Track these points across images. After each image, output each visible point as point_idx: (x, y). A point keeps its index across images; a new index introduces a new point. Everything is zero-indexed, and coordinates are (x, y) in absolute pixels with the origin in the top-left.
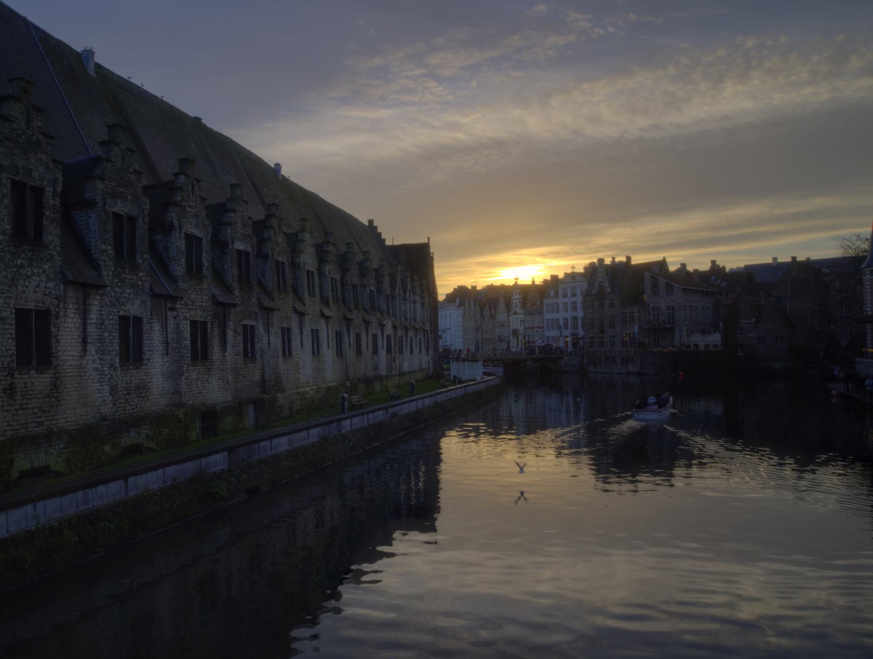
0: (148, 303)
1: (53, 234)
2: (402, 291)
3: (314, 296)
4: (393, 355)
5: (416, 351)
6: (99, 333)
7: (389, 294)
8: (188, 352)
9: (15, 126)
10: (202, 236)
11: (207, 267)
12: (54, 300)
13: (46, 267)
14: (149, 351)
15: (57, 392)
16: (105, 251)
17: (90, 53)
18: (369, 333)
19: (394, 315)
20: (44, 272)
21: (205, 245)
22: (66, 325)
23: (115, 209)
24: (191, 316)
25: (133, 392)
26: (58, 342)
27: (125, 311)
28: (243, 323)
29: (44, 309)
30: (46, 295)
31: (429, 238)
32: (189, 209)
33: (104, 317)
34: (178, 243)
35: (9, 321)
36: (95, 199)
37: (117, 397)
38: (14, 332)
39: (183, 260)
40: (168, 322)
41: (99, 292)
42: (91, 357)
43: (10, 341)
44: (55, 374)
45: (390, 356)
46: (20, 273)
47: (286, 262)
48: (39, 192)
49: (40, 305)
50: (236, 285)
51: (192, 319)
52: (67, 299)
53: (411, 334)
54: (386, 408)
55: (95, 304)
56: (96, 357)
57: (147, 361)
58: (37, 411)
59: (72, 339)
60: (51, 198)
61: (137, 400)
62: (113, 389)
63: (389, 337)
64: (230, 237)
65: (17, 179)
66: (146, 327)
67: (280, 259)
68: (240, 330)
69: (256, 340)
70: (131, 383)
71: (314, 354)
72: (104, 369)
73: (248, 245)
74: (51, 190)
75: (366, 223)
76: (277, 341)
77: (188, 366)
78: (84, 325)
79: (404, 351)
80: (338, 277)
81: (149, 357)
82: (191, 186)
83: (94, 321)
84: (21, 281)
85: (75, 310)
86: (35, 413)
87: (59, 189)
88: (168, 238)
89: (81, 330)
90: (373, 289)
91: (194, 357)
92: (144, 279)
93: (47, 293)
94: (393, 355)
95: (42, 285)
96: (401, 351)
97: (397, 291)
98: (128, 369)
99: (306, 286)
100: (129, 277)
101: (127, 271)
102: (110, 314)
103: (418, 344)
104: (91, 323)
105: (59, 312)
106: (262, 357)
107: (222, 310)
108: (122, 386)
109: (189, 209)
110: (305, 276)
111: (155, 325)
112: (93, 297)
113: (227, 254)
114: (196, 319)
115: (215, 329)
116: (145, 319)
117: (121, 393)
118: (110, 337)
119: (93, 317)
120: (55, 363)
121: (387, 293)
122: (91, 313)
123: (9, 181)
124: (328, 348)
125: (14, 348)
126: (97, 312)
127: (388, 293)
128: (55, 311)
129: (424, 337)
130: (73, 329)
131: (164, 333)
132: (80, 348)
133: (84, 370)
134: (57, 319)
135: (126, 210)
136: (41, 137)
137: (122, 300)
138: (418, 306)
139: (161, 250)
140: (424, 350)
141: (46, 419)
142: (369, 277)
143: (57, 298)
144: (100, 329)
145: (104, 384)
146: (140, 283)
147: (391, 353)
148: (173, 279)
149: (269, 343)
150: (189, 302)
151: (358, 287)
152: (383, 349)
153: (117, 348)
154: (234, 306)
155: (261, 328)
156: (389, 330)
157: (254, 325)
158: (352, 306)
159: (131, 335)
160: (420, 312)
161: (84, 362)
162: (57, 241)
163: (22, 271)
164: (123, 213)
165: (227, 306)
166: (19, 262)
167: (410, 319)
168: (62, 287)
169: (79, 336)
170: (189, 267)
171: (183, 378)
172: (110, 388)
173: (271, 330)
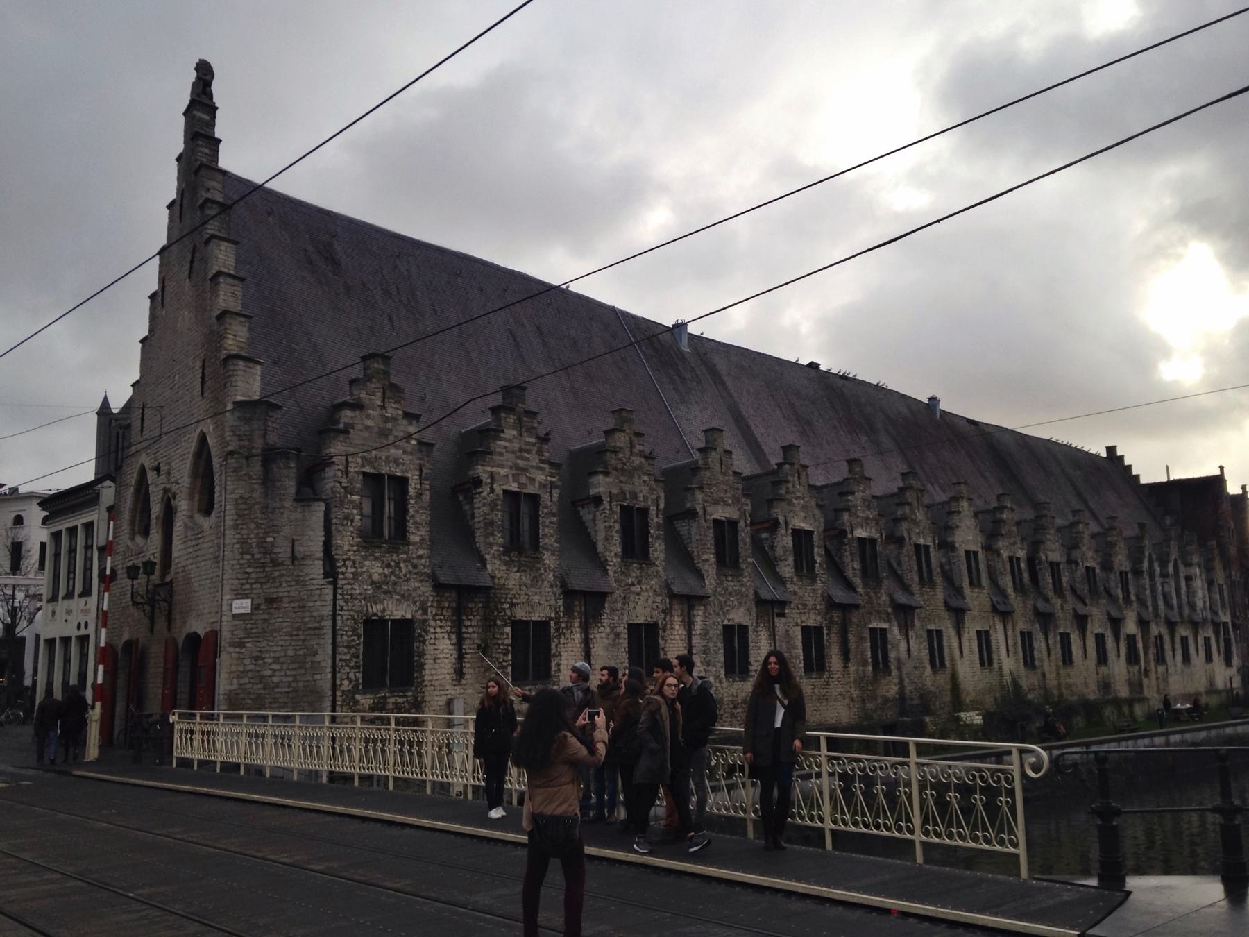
0: (754, 610)
1: (658, 549)
3: (980, 586)
4: (1143, 668)
7: (1128, 569)
8: (800, 662)
11: (820, 564)
13: (653, 582)
16: (707, 560)
17: (681, 326)
19: (1141, 602)
20: (651, 588)
22: (672, 637)
24: (802, 622)
27: (729, 620)
28: (871, 626)
31: (1222, 468)
32: (794, 501)
33: (708, 628)
34: (785, 541)
35: (622, 635)
39: (791, 560)
40: (777, 629)
41: (703, 603)
43: (624, 654)
45: (1137, 667)
47: (932, 545)
48: (644, 512)
49: (649, 619)
50: (858, 581)
51: (803, 624)
53: (1183, 631)
54: (1088, 745)
55: (699, 613)
56: (702, 669)
63: (1131, 639)
64: (848, 524)
65: (625, 504)
66: (751, 636)
67: (922, 541)
68: (867, 634)
69: (890, 647)
70: (737, 696)
71: (982, 664)
73: (873, 531)
74: (655, 508)
75: (1104, 454)
76: (919, 648)
80: (1021, 554)
82: (796, 475)
83: (698, 632)
85: (681, 622)
87: (662, 506)
90: (1092, 564)
92: (748, 584)
94: (1143, 668)
95: (650, 601)
96: (1161, 659)
97: (1146, 564)
98: (734, 681)
99: (965, 572)
100: (732, 584)
101: (730, 578)
102: (714, 624)
106: (899, 669)
107: (839, 611)
109: (794, 501)
110: (964, 560)
111: (762, 633)
112: (697, 608)
114: (809, 624)
116: (750, 629)
119: (698, 627)
121: (1123, 568)
123: (619, 507)
124: (1008, 656)
125: (627, 661)
129: (1217, 633)
130: (679, 641)
134: (664, 630)
135: (727, 515)
136: (643, 460)
139: (766, 548)
142: (1084, 549)
146: (744, 589)
148: (781, 581)
149: (909, 650)
150: (800, 606)
151: (1061, 567)
152: (1119, 656)
153: (722, 659)
154: (857, 607)
155: (896, 630)
156: (1131, 627)
157: (886, 629)
158: (1051, 594)
159: (736, 645)
160: (1204, 597)
162: (662, 556)
163: (633, 588)
164: (723, 519)
165: (846, 608)
166: (630, 581)
167: (1180, 607)
168: (668, 601)
170: (798, 567)
173: (911, 633)
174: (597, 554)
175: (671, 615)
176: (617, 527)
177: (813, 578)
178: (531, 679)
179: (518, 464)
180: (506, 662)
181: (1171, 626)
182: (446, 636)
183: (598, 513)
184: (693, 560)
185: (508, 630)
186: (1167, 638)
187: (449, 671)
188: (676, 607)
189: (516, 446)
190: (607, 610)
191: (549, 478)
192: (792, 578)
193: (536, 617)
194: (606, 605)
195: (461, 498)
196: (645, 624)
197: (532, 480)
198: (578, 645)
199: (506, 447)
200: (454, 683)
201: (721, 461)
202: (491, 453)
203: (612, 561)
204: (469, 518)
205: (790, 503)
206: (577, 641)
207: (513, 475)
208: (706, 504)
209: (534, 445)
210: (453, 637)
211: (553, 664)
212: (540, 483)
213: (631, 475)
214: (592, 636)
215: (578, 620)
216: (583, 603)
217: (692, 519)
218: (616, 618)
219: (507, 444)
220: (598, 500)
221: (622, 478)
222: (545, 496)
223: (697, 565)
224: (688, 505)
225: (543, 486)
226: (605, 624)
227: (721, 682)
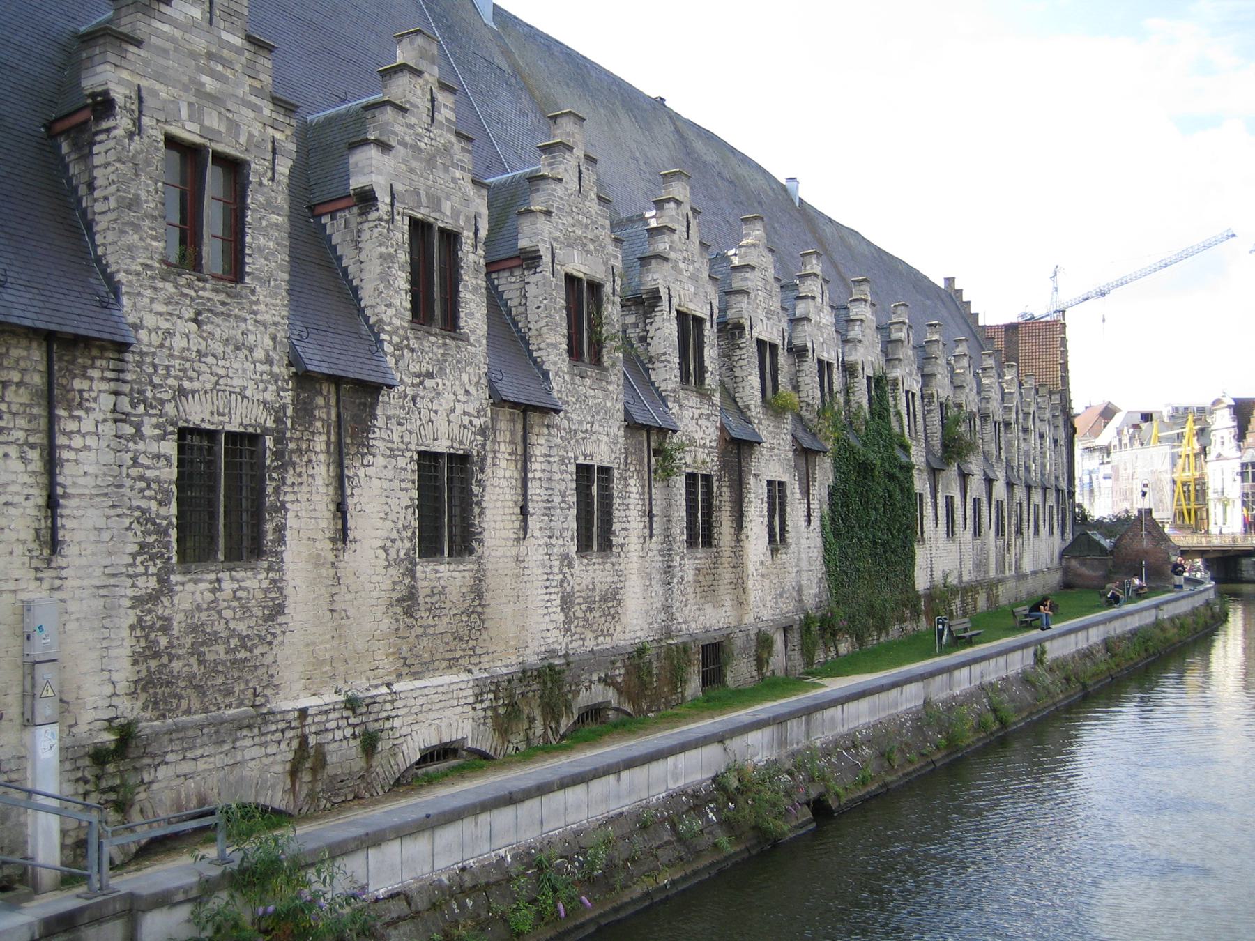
0: (621, 440)
2: (1021, 416)
5: (1044, 532)
6: (547, 497)
9: (413, 120)
10: (702, 316)
12: (478, 437)
13: (465, 377)
14: (623, 529)
15: (480, 605)
16: (554, 346)
18: (968, 497)
21: (710, 333)
23: (570, 269)
25: (597, 605)
26: (482, 513)
29: (461, 452)
30: (465, 427)
32: (682, 265)
34: (665, 330)
36: (538, 251)
37: (571, 614)
38: (415, 494)
42: (535, 541)
44: (478, 570)
46: (425, 388)
47: (835, 362)
48: (451, 238)
49: (456, 445)
51: (688, 470)
52: (498, 432)
53: (1037, 498)
57: (619, 550)
58: (449, 638)
59: (504, 507)
60: (471, 249)
61: (603, 619)
62: (566, 602)
64: (746, 316)
65: (419, 216)
66: (617, 485)
67: (825, 357)
69: (788, 509)
70: (594, 589)
72: (553, 563)
75: (941, 284)
77: (682, 558)
78: (525, 482)
79: (1025, 531)
80: (916, 388)
81: (623, 541)
82: (685, 224)
83: (538, 475)
84: (426, 401)
85: (510, 454)
86: (447, 644)
87: (483, 233)
88: (648, 321)
89: (519, 490)
91: (691, 542)
93: (466, 422)
95: (459, 409)
96: (1019, 532)
103: (1047, 519)
104: (534, 478)
105: (484, 459)
108: (579, 594)
111: (632, 482)
112: (536, 430)
113: (741, 348)
114: (695, 471)
115: (724, 489)
117: (577, 608)
118: (563, 505)
119: (537, 466)
120: (479, 551)
122: (533, 459)
123: (407, 220)
126: (542, 459)
127: (999, 418)
128: (478, 455)
130: (507, 490)
131: (647, 496)
132: (517, 524)
133: (522, 565)
134: (482, 470)
136: (453, 139)
137: (582, 435)
138: (1048, 442)
140: (1057, 531)
141: (462, 653)
143: (482, 431)
144: (547, 489)
145: (552, 590)
147: (1003, 535)
161: (523, 551)
162: (482, 328)
164: (581, 275)
169: (515, 502)
171: (675, 580)
172: (562, 598)
174: (361, 310)
175: (494, 441)
176: (403, 257)
177: (704, 395)
178: (221, 557)
179: (203, 85)
180: (165, 518)
181: (1029, 487)
182: (13, 451)
183: (366, 226)
184: (528, 344)
185: (170, 447)
186: (1025, 505)
187: (22, 536)
188: (502, 425)
189: (200, 43)
190: (380, 422)
191: (270, 131)
192: (674, 391)
193: (234, 427)
194: (379, 411)
195: (65, 148)
196: (450, 456)
197: (234, 126)
198: (322, 489)
199: (172, 39)
200: (35, 563)
201: (580, 172)
202: (138, 43)
203: (390, 324)
204: (82, 190)
205: (675, 267)
206: (319, 481)
207: (190, 104)
208: (555, 245)
209: (238, 51)
210: (34, 455)
211: (269, 527)
212: (251, 136)
213: (431, 161)
214: (348, 472)
215: (324, 437)
216: (333, 402)
217: (529, 268)
218: (396, 439)
219: (178, 33)
220: (366, 199)
221: (415, 164)
222: (258, 167)
223: (535, 354)
224: (523, 243)
225: (253, 144)
226: (374, 450)
227: (570, 565)
